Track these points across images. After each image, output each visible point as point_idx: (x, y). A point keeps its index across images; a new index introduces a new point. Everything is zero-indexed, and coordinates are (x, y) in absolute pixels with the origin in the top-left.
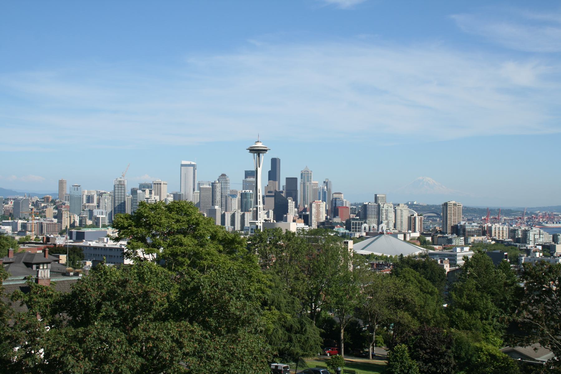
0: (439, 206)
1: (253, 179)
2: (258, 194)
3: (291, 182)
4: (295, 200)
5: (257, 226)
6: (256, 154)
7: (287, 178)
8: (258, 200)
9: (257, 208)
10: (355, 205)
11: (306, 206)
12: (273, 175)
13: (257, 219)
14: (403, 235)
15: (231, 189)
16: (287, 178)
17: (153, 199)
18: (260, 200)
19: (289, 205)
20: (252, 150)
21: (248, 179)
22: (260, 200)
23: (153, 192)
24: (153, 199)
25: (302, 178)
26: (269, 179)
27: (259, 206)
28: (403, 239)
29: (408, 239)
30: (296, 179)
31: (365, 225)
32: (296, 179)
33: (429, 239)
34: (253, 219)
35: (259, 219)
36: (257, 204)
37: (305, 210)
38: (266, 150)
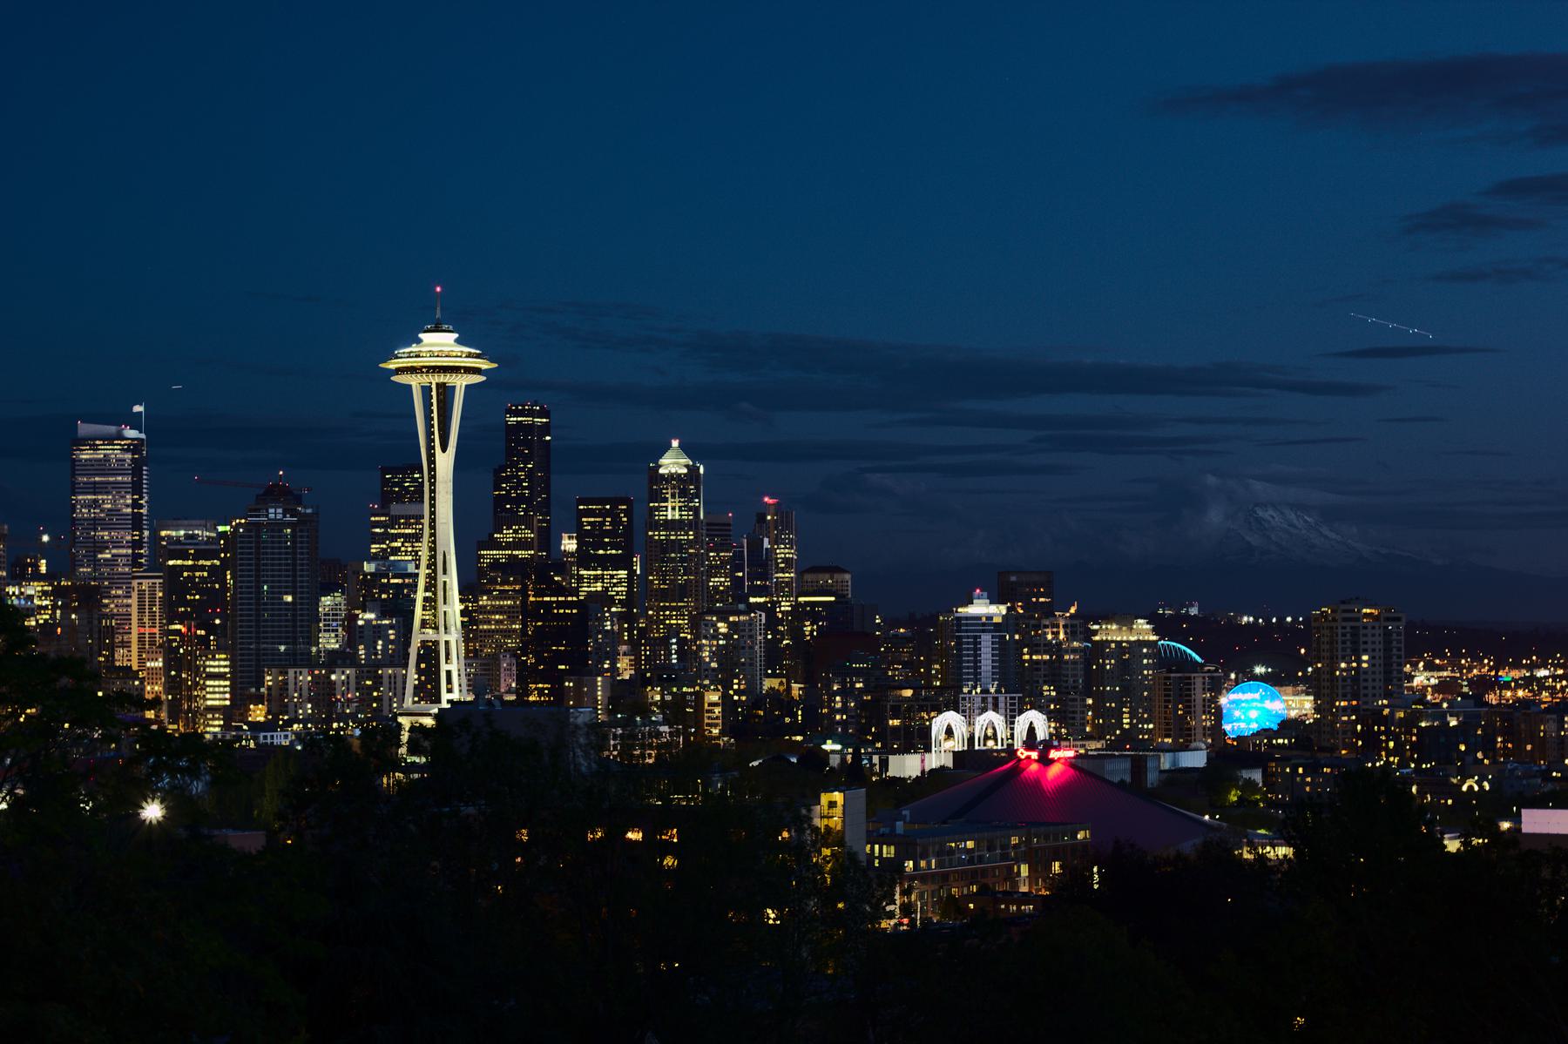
2: (441, 578)
9: (436, 643)
14: (1127, 765)
26: (495, 512)
27: (443, 638)
28: (1128, 779)
29: (1152, 778)
31: (951, 718)
35: (445, 696)
36: (436, 628)
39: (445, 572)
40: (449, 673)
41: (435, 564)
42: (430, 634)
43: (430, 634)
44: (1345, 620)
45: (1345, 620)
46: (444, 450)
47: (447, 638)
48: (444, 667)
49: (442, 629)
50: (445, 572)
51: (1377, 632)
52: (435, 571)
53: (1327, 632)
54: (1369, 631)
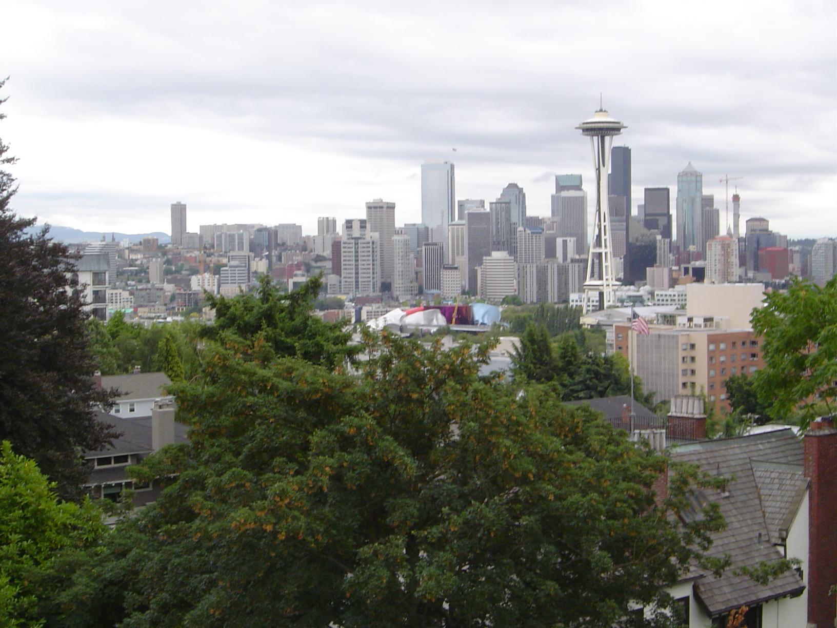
1: (572, 193)
3: (657, 196)
4: (667, 233)
5: (601, 295)
6: (595, 138)
7: (646, 190)
9: (600, 254)
11: (692, 248)
12: (620, 183)
13: (601, 278)
15: (530, 213)
16: (646, 190)
17: (368, 239)
18: (607, 237)
19: (658, 244)
21: (565, 194)
22: (607, 237)
23: (368, 225)
24: (368, 239)
25: (679, 191)
27: (603, 250)
32: (667, 190)
35: (604, 278)
37: (689, 257)
38: (618, 129)
42: (598, 250)
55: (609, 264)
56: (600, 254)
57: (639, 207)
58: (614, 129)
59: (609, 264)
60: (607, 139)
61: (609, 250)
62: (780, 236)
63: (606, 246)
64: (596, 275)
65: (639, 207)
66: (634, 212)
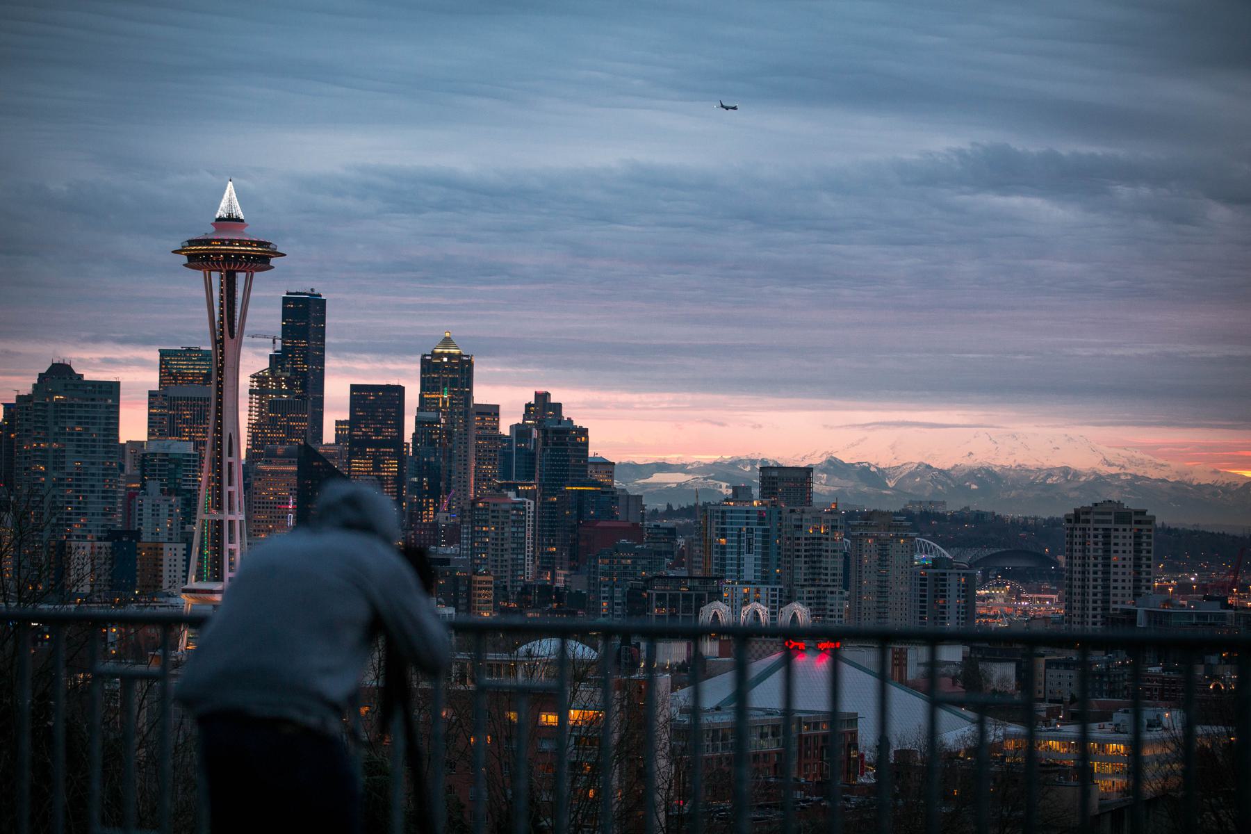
0: (1053, 522)
3: (376, 403)
8: (227, 489)
9: (220, 523)
10: (669, 512)
16: (354, 388)
20: (200, 256)
27: (226, 517)
30: (397, 392)
32: (400, 390)
33: (1002, 674)
34: (199, 578)
36: (220, 509)
39: (230, 455)
40: (232, 553)
41: (220, 446)
42: (216, 515)
43: (216, 515)
44: (1097, 521)
45: (1097, 521)
46: (232, 336)
47: (231, 517)
48: (227, 546)
49: (226, 509)
50: (230, 455)
51: (1128, 534)
52: (220, 453)
53: (1078, 533)
54: (1121, 533)
55: (236, 546)
56: (220, 523)
57: (338, 423)
58: (260, 257)
59: (236, 546)
60: (241, 277)
61: (239, 516)
62: (628, 496)
63: (231, 508)
64: (207, 572)
65: (338, 423)
66: (329, 436)
